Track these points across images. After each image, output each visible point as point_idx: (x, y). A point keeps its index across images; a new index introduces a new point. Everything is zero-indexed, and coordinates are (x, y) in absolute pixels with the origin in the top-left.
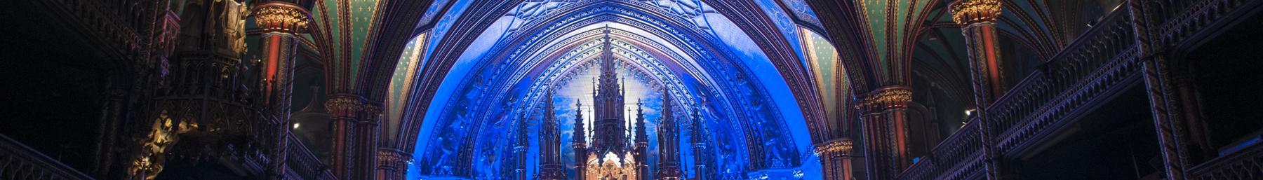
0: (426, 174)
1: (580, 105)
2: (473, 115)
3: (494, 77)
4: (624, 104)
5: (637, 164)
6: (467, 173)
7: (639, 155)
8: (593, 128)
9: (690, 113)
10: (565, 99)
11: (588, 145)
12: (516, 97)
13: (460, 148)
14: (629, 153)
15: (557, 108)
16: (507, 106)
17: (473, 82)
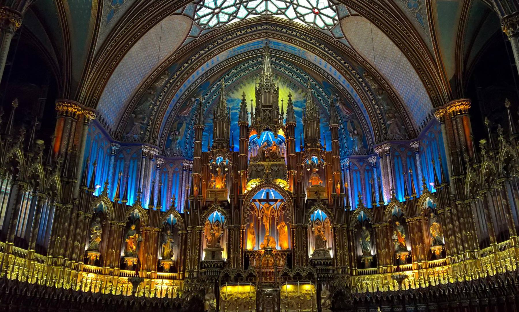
0: (119, 140)
1: (245, 96)
2: (160, 98)
3: (178, 72)
4: (278, 97)
5: (287, 138)
6: (154, 142)
7: (289, 132)
8: (254, 113)
9: (327, 109)
10: (236, 100)
11: (250, 123)
12: (198, 95)
13: (148, 122)
14: (281, 129)
15: (230, 106)
16: (192, 101)
17: (161, 75)
